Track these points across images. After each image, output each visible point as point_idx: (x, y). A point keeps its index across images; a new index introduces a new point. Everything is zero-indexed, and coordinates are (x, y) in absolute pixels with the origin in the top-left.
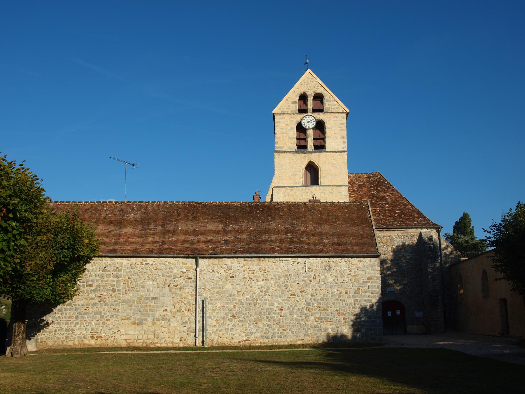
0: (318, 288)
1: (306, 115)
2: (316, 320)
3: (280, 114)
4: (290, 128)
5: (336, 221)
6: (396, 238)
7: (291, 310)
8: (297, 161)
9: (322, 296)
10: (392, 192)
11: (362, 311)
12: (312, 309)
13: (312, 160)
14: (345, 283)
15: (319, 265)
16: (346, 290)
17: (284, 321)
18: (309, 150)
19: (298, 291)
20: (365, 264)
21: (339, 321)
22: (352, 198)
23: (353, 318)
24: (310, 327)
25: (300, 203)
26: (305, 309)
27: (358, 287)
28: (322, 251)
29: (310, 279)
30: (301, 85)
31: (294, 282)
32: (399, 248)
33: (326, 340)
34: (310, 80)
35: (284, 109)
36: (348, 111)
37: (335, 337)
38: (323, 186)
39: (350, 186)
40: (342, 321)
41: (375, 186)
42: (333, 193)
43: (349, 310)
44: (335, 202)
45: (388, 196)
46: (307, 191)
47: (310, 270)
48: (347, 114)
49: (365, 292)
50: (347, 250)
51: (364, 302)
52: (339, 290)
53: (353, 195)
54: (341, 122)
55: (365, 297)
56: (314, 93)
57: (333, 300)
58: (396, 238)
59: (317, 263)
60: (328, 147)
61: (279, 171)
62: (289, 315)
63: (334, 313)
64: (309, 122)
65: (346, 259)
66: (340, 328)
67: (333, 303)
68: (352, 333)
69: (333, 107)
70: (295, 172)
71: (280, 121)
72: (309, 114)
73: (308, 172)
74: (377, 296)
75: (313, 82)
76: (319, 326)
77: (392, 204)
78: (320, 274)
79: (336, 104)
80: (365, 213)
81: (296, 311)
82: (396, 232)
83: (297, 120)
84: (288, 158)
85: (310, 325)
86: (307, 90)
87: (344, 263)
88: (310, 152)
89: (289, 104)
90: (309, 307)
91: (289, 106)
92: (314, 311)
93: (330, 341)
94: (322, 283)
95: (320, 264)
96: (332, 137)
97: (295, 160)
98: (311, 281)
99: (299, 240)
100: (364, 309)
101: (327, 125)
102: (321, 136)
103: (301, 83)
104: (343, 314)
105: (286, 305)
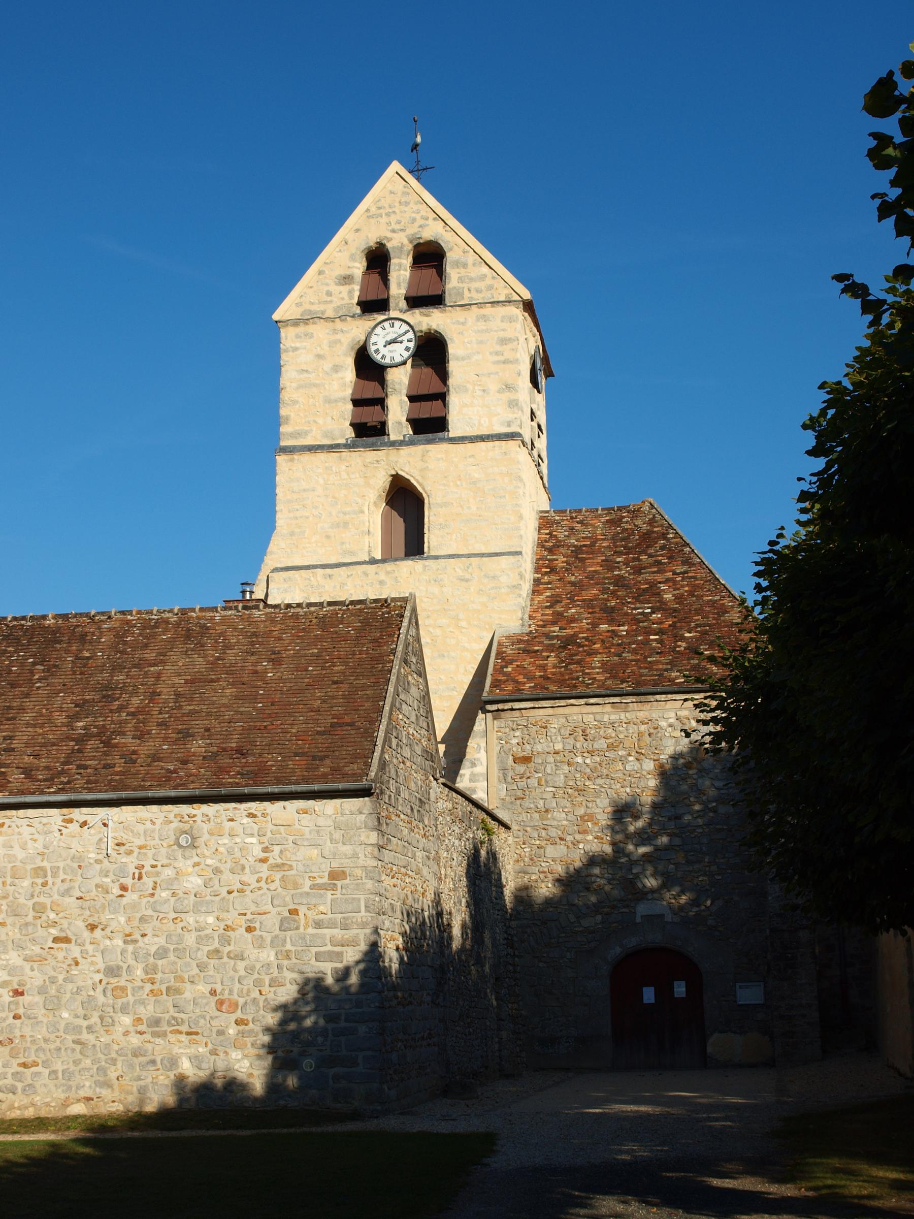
0: (150, 912)
1: (382, 317)
2: (140, 1028)
3: (296, 323)
4: (330, 365)
5: (266, 672)
6: (670, 726)
7: (53, 992)
8: (352, 476)
9: (161, 941)
10: (685, 568)
11: (304, 995)
12: (123, 989)
13: (401, 473)
14: (248, 893)
15: (153, 831)
16: (249, 916)
17: (27, 1031)
18: (393, 437)
19: (81, 925)
20: (321, 821)
21: (221, 1033)
22: (541, 594)
23: (272, 1019)
24: (117, 1052)
25: (168, 615)
26: (100, 989)
27: (292, 907)
28: (169, 779)
29: (122, 880)
30: (368, 217)
31: (67, 893)
32: (681, 761)
33: (171, 1100)
34: (397, 200)
36: (527, 295)
37: (205, 1089)
38: (436, 558)
39: (546, 553)
40: (231, 1031)
41: (629, 550)
42: (467, 581)
43: (257, 990)
44: (289, 606)
45: (667, 581)
46: (382, 576)
47: (122, 849)
48: (528, 306)
49: (318, 925)
50: (258, 774)
51: (313, 962)
52: (223, 920)
53: (549, 583)
54: (502, 334)
55: (319, 941)
56: (411, 242)
57: (202, 955)
58: (670, 726)
59: (148, 823)
60: (456, 427)
61: (292, 515)
62: (44, 1011)
63: (205, 1001)
64: (394, 341)
65: (253, 806)
66: (222, 1055)
67: (202, 967)
68: (267, 1075)
69: (477, 285)
70: (345, 514)
71: (298, 345)
72: (393, 314)
73: (394, 513)
74: (362, 937)
75: (407, 204)
76: (146, 1051)
77: (675, 610)
78: (159, 864)
79: (485, 276)
80: (381, 637)
81: (68, 995)
82: (670, 705)
83: (353, 340)
84: (320, 471)
85: (116, 1047)
86: (389, 235)
87: (246, 820)
89: (327, 285)
90: (114, 981)
91: (329, 294)
92: (133, 995)
93: (186, 1106)
94: (164, 894)
95: (157, 827)
96: (470, 387)
98: (124, 888)
99: (107, 743)
100: (311, 985)
101: (453, 350)
102: (435, 386)
103: (368, 210)
104: (236, 1005)
105: (34, 978)
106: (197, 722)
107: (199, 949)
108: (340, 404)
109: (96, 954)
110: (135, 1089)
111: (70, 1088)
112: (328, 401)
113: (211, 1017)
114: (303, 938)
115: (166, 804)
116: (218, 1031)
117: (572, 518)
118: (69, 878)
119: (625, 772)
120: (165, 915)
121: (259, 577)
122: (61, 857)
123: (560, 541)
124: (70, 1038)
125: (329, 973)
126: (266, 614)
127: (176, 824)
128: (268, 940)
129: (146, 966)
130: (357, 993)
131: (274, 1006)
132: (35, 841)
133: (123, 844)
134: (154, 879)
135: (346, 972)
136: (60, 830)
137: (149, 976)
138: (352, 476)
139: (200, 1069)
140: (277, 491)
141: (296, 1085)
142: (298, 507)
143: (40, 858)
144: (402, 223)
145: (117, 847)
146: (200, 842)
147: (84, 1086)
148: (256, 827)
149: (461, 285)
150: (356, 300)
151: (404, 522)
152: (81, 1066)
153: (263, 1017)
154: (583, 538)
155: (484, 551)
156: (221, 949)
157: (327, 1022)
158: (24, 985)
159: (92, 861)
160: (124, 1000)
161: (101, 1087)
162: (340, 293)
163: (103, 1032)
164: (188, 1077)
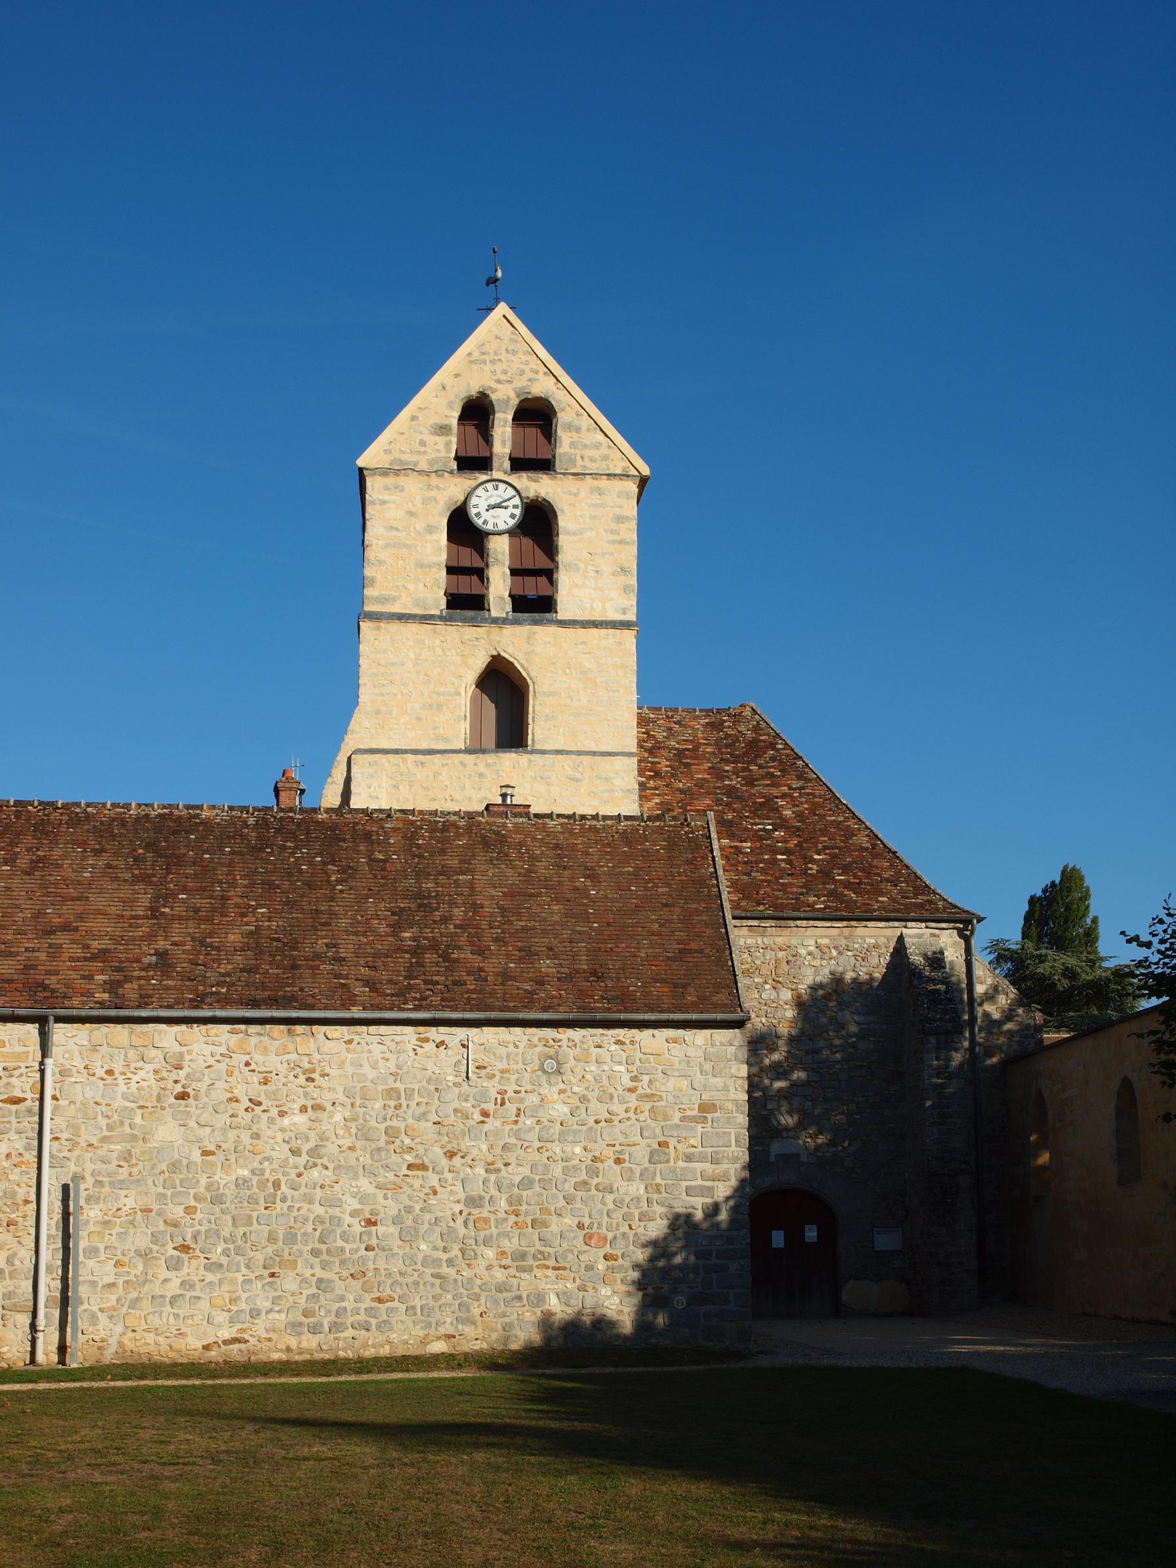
0: (513, 1140)
1: (484, 477)
2: (504, 1262)
3: (385, 472)
4: (423, 525)
5: (586, 889)
6: (810, 954)
7: (410, 1223)
8: (448, 653)
9: (526, 1171)
10: (801, 783)
11: (674, 1230)
12: (486, 1221)
13: (503, 654)
14: (616, 1123)
15: (517, 1055)
16: (618, 1148)
17: (381, 1264)
18: (494, 613)
19: (439, 1151)
20: (691, 1052)
21: (589, 1268)
22: (649, 800)
23: (641, 1255)
24: (480, 1287)
25: (453, 818)
26: (460, 1220)
27: (661, 1139)
28: (532, 1001)
29: (484, 1106)
30: (470, 362)
31: (423, 1116)
32: (821, 992)
33: (537, 1338)
34: (504, 347)
35: (403, 452)
36: (646, 470)
37: (572, 1328)
38: (543, 752)
39: (646, 755)
40: (600, 1267)
42: (577, 780)
43: (626, 1224)
44: (583, 817)
45: (783, 796)
46: (482, 768)
47: (483, 1072)
48: (643, 482)
49: (689, 1158)
50: (624, 1000)
51: (684, 1196)
52: (591, 1151)
53: (656, 788)
54: (618, 511)
55: (689, 1176)
56: (518, 396)
57: (569, 1187)
58: (810, 954)
59: (511, 1046)
61: (377, 691)
62: (399, 1242)
63: (572, 1235)
64: (498, 506)
65: (620, 1033)
66: (591, 1292)
67: (569, 1200)
68: (637, 1313)
69: (588, 453)
70: (438, 694)
71: (386, 498)
72: (496, 474)
73: (485, 697)
74: (732, 1172)
75: (514, 352)
76: (511, 1286)
77: (798, 829)
78: (523, 1090)
79: (600, 444)
80: (695, 858)
81: (426, 1226)
82: (810, 932)
83: (450, 499)
84: (411, 643)
85: (479, 1282)
86: (494, 385)
87: (613, 1047)
88: (495, 621)
89: (421, 433)
90: (475, 1211)
91: (423, 443)
92: (497, 1227)
93: (554, 1344)
94: (528, 1122)
95: (520, 1050)
96: (581, 565)
97: (439, 651)
98: (485, 1114)
99: (446, 957)
100: (682, 1220)
101: (565, 522)
102: (542, 562)
103: (470, 354)
104: (605, 1239)
105: (389, 1207)
106: (536, 940)
107: (566, 1180)
108: (434, 570)
109: (455, 1182)
110: (499, 1326)
111: (429, 1325)
112: (420, 565)
113: (579, 1252)
114: (674, 1171)
115: (530, 1027)
116: (586, 1267)
117: (668, 717)
118: (425, 1101)
119: (761, 1001)
120: (529, 1144)
121: (338, 758)
122: (416, 1078)
123: (660, 743)
124: (428, 1271)
125: (700, 1207)
126: (561, 824)
127: (540, 1049)
128: (638, 1173)
129: (510, 1196)
130: (728, 1230)
131: (645, 1242)
132: (387, 1060)
133: (485, 1068)
134: (517, 1105)
135: (716, 1207)
136: (414, 1050)
137: (513, 1208)
138: (448, 653)
139: (569, 1306)
140: (361, 662)
141: (667, 1323)
142: (385, 682)
143: (393, 1078)
144: (509, 374)
145: (477, 1071)
146: (566, 1068)
147: (444, 1323)
148: (624, 1055)
149: (572, 451)
150: (453, 454)
151: (496, 708)
152: (441, 1302)
153: (633, 1252)
154: (684, 740)
155: (594, 748)
156: (590, 1180)
157: (697, 1258)
158: (377, 1215)
159: (450, 1084)
160: (487, 1232)
161: (463, 1324)
162: (436, 444)
163: (464, 1266)
164: (556, 1314)
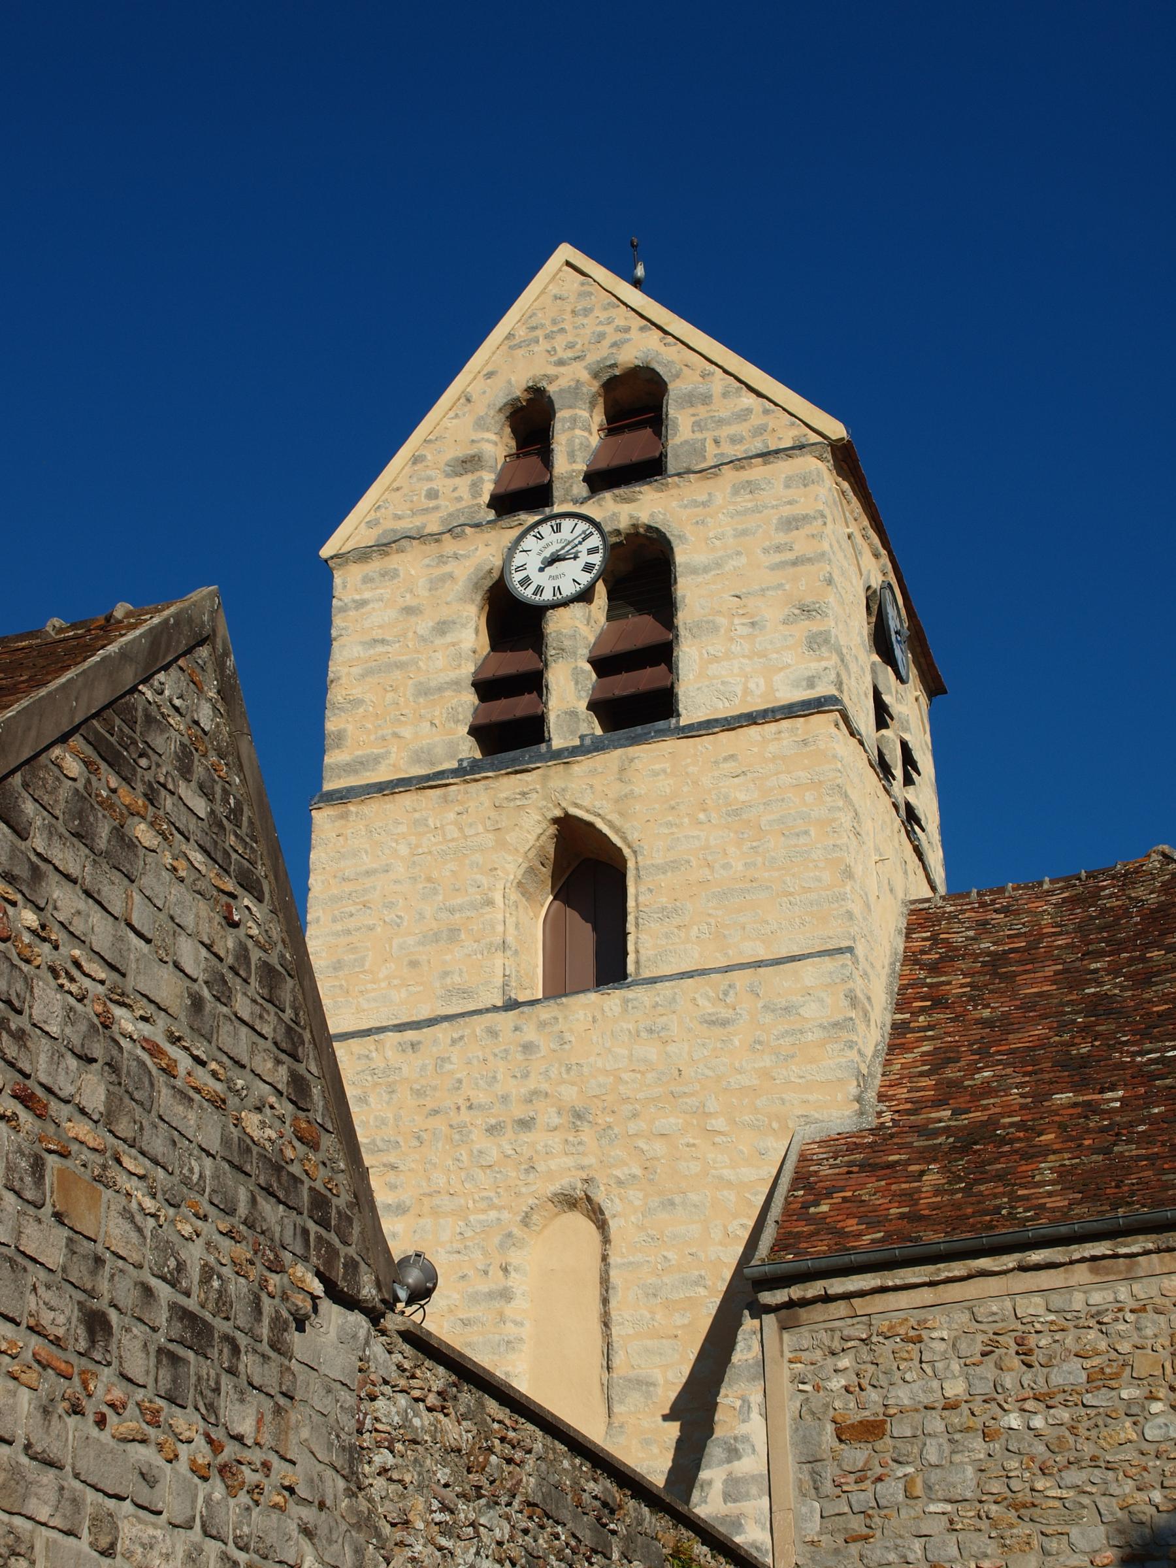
3: (363, 555)
8: (469, 832)
13: (573, 811)
18: (557, 743)
35: (399, 518)
36: (836, 430)
38: (653, 981)
41: (1117, 947)
42: (724, 1023)
46: (530, 1034)
53: (930, 1027)
54: (787, 511)
60: (693, 706)
61: (338, 927)
70: (452, 911)
71: (367, 595)
72: (557, 509)
73: (573, 916)
75: (587, 312)
79: (749, 411)
84: (403, 829)
86: (552, 370)
88: (557, 755)
91: (432, 494)
96: (722, 621)
97: (452, 832)
103: (510, 336)
108: (448, 693)
112: (424, 691)
117: (983, 905)
119: (1145, 1447)
123: (957, 949)
138: (469, 832)
140: (311, 881)
142: (353, 909)
144: (578, 346)
149: (698, 436)
150: (486, 498)
151: (595, 929)
154: (1009, 936)
155: (763, 954)
162: (455, 489)
